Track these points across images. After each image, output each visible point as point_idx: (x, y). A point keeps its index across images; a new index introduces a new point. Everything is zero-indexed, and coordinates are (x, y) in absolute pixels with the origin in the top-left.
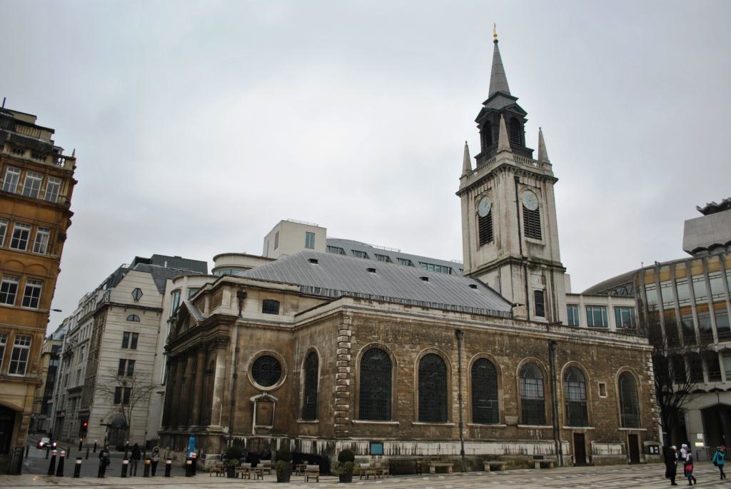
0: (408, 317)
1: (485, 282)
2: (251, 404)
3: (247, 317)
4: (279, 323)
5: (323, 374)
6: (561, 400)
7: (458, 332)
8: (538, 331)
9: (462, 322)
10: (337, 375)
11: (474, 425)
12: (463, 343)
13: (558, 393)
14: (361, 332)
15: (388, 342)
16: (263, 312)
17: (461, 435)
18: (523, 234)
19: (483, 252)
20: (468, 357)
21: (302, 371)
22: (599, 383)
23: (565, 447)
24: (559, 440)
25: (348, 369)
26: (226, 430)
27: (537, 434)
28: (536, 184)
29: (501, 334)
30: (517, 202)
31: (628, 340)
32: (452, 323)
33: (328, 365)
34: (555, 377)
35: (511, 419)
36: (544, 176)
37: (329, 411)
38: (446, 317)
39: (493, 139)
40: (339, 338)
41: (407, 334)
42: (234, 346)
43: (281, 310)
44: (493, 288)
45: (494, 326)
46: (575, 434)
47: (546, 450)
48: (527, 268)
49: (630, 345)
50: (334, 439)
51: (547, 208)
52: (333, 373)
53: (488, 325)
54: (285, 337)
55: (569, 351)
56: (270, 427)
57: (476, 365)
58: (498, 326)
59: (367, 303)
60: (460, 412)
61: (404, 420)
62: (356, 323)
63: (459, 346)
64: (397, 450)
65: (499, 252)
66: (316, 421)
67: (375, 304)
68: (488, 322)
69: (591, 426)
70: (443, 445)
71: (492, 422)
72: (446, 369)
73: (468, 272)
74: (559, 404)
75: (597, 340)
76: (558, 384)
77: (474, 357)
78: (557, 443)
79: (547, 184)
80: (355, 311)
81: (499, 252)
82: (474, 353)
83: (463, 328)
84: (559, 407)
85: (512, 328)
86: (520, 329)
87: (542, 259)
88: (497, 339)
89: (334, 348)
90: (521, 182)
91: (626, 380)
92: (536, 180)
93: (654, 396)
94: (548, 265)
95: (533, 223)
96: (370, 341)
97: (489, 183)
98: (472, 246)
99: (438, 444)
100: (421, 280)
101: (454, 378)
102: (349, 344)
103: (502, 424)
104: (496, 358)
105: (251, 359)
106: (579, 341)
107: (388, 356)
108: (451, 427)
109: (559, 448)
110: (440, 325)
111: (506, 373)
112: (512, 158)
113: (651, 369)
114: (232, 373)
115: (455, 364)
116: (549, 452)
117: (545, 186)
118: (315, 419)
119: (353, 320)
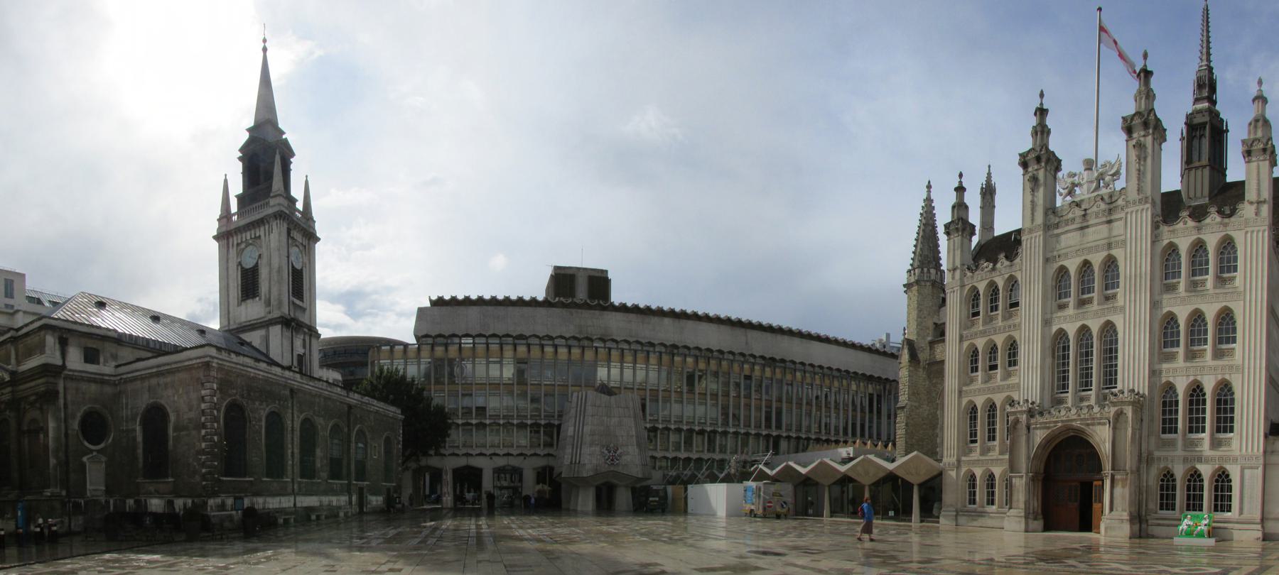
5: (176, 429)
7: (292, 391)
10: (203, 432)
14: (225, 386)
29: (320, 396)
40: (203, 392)
64: (253, 504)
67: (233, 355)
70: (283, 499)
77: (302, 417)
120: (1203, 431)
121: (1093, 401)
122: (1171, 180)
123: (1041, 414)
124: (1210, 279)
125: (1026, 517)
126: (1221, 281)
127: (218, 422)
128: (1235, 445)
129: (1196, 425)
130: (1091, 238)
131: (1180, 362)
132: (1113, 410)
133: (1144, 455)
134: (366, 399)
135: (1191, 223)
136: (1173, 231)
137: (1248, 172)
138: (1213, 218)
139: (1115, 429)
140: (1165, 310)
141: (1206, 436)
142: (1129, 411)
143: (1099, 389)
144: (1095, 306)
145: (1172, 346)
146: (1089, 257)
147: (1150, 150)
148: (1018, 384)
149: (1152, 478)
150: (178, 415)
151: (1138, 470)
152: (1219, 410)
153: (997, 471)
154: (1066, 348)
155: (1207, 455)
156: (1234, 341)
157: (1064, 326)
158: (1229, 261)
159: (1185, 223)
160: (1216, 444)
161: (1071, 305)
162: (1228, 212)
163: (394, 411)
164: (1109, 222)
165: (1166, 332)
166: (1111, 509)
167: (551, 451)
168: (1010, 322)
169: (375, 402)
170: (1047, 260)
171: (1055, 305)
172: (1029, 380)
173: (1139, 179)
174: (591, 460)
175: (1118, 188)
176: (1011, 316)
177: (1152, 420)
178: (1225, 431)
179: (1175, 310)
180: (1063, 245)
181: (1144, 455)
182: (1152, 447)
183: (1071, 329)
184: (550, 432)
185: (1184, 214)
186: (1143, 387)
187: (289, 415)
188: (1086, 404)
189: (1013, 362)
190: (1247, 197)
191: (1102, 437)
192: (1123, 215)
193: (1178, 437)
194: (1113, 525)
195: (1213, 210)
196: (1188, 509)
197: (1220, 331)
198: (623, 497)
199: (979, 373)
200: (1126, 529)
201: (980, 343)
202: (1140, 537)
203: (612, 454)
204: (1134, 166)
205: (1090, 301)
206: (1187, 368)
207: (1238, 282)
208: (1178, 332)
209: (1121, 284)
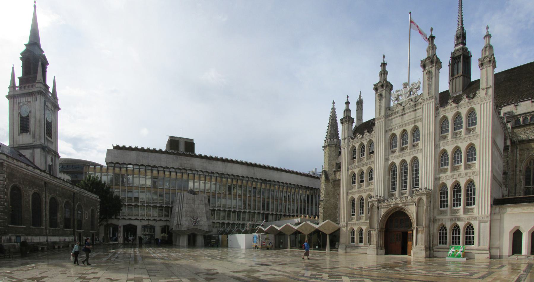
7: (45, 183)
25: (6, 197)
95: (50, 130)
120: (460, 205)
121: (407, 194)
122: (444, 85)
123: (384, 201)
124: (463, 130)
125: (377, 249)
126: (468, 131)
127: (7, 195)
128: (476, 211)
129: (456, 203)
130: (407, 119)
131: (449, 173)
132: (417, 198)
133: (432, 218)
134: (82, 190)
135: (454, 105)
136: (445, 110)
137: (482, 75)
138: (465, 100)
139: (418, 207)
140: (441, 149)
141: (461, 208)
142: (424, 198)
143: (410, 188)
144: (408, 150)
145: (445, 165)
146: (405, 128)
147: (434, 74)
148: (374, 188)
149: (436, 229)
151: (429, 225)
152: (468, 195)
153: (364, 228)
154: (395, 171)
155: (462, 216)
156: (475, 160)
157: (394, 161)
158: (472, 120)
159: (451, 105)
160: (466, 211)
161: (397, 151)
162: (472, 96)
163: (95, 197)
164: (415, 110)
165: (442, 159)
166: (416, 244)
167: (168, 219)
168: (370, 161)
169: (87, 192)
170: (386, 131)
171: (390, 151)
172: (378, 186)
173: (429, 88)
174: (186, 223)
175: (419, 94)
176: (370, 158)
177: (435, 202)
178: (471, 205)
179: (446, 148)
180: (394, 123)
181: (432, 218)
182: (436, 214)
183: (398, 162)
184: (167, 210)
185: (450, 101)
186: (431, 186)
187: (44, 195)
188: (404, 196)
189: (371, 179)
190: (481, 86)
191: (412, 211)
192: (421, 106)
193: (448, 209)
194: (417, 251)
195: (464, 96)
196: (453, 244)
197: (468, 155)
198: (200, 240)
199: (356, 184)
200: (423, 254)
201: (356, 171)
202: (430, 257)
203: (195, 220)
204: (427, 83)
205: (406, 148)
206: (452, 175)
207: (477, 130)
208: (448, 159)
209: (421, 139)
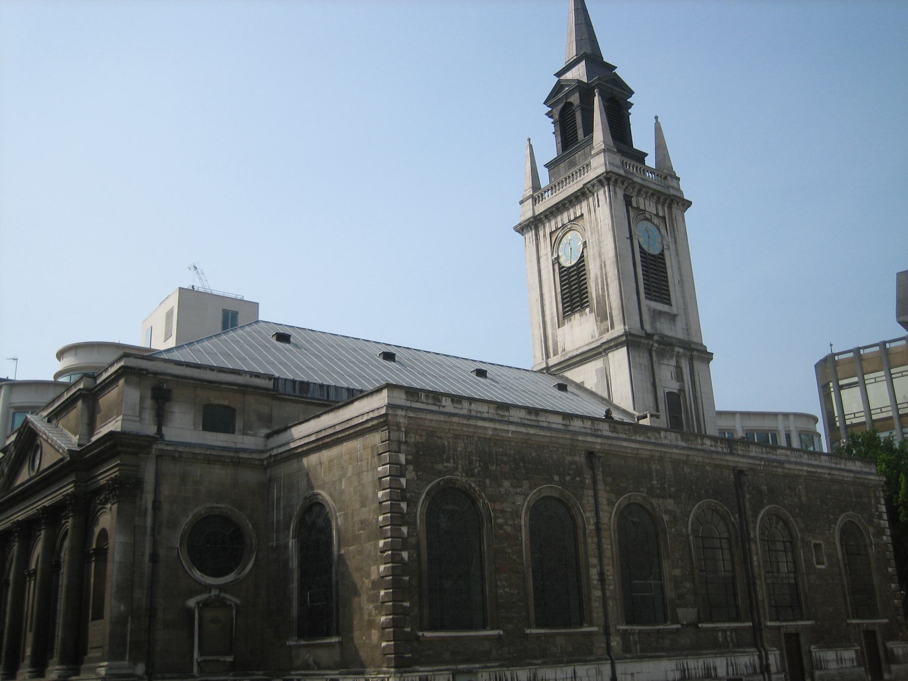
0: (505, 427)
1: (578, 382)
2: (190, 612)
3: (173, 439)
4: (237, 450)
6: (760, 575)
7: (590, 454)
8: (718, 453)
9: (598, 436)
11: (629, 627)
12: (600, 477)
13: (755, 563)
15: (473, 475)
16: (204, 429)
17: (609, 649)
18: (643, 295)
19: (572, 328)
20: (611, 503)
21: (292, 543)
22: (814, 542)
23: (774, 659)
24: (763, 646)
25: (405, 530)
26: (140, 669)
27: (729, 639)
28: (657, 209)
29: (661, 459)
30: (631, 238)
31: (847, 468)
32: (580, 438)
33: (356, 527)
34: (749, 534)
35: (687, 614)
36: (670, 196)
37: (366, 617)
38: (571, 428)
39: (580, 132)
41: (505, 459)
42: (149, 498)
43: (239, 425)
44: (594, 390)
45: (649, 443)
46: (785, 634)
47: (746, 666)
48: (654, 354)
49: (852, 475)
50: (385, 673)
51: (677, 250)
52: (369, 539)
53: (639, 442)
54: (250, 477)
55: (764, 488)
56: (229, 659)
57: (622, 515)
58: (655, 444)
59: (430, 401)
60: (605, 605)
61: (510, 626)
62: (412, 439)
63: (594, 482)
65: (603, 326)
66: (335, 640)
68: (638, 438)
69: (808, 620)
71: (656, 623)
72: (575, 527)
73: (544, 365)
74: (758, 582)
75: (806, 468)
76: (753, 546)
77: (621, 501)
78: (760, 652)
79: (675, 211)
80: (411, 415)
81: (603, 326)
82: (619, 494)
83: (598, 447)
84: (758, 588)
85: (677, 447)
86: (691, 449)
87: (673, 338)
88: (653, 467)
89: (369, 490)
90: (634, 205)
91: (850, 532)
92: (657, 202)
93: (893, 562)
94: (685, 348)
96: (440, 473)
97: (578, 207)
98: (548, 318)
99: (569, 670)
100: (474, 375)
101: (589, 540)
102: (403, 481)
103: (673, 623)
104: (654, 501)
105: (185, 521)
106: (780, 470)
107: (474, 502)
108: (590, 634)
109: (765, 663)
110: (561, 441)
111: (673, 530)
112: (619, 164)
113: (885, 516)
114: (147, 552)
115: (589, 515)
116: (750, 670)
117: (670, 213)
118: (328, 635)
119: (407, 434)
127: (411, 524)
150: (346, 515)
